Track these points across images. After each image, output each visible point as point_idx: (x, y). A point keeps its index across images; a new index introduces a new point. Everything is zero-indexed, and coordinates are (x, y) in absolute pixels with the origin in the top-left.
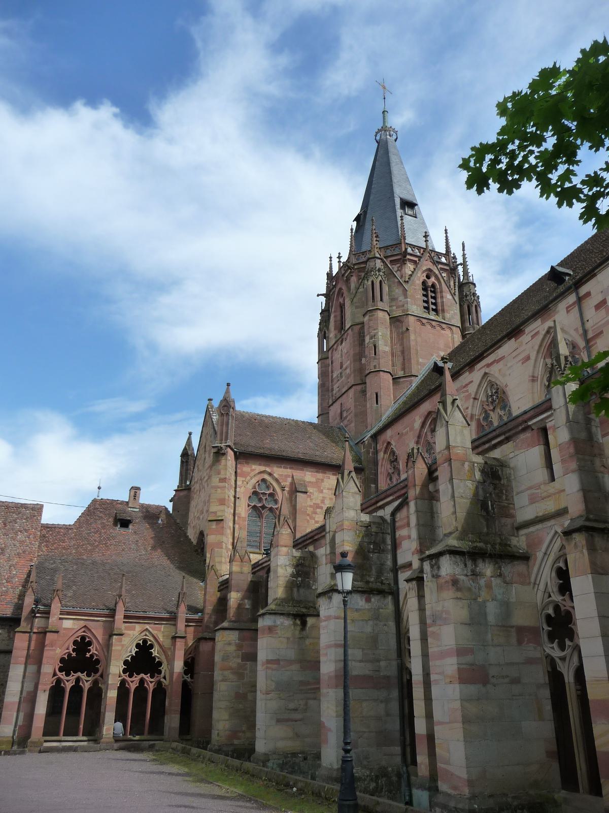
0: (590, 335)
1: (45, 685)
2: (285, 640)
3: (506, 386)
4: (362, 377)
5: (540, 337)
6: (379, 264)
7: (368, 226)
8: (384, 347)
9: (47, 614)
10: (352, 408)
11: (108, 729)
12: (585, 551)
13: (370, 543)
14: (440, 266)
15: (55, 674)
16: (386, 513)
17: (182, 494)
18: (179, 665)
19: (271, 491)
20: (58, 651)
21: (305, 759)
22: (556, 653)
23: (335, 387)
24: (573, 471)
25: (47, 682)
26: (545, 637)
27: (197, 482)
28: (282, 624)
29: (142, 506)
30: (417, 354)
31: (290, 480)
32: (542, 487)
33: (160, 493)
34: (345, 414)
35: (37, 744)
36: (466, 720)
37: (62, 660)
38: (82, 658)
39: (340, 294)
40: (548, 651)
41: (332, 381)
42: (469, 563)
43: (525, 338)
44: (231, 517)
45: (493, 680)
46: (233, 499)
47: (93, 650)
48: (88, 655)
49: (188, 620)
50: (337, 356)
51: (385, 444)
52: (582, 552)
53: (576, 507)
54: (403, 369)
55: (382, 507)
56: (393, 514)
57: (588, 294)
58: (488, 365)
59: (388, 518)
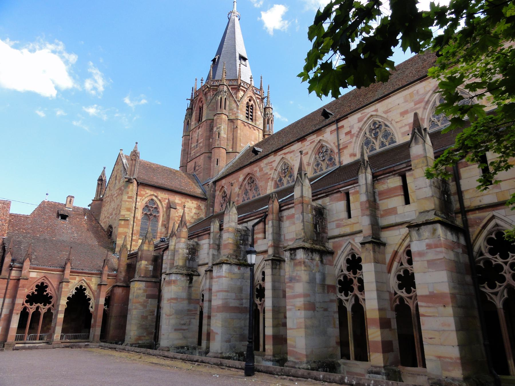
0: (341, 147)
1: (18, 310)
2: (181, 288)
3: (294, 166)
4: (210, 149)
5: (315, 144)
6: (225, 89)
7: (220, 66)
8: (223, 135)
9: (21, 269)
10: (202, 166)
11: (57, 336)
12: (372, 252)
13: (241, 240)
14: (257, 96)
15: (23, 304)
16: (250, 225)
17: (97, 202)
18: (102, 301)
19: (155, 206)
20: (26, 290)
21: (188, 349)
22: (343, 298)
23: (192, 152)
24: (367, 215)
25: (18, 309)
26: (337, 290)
27: (108, 197)
28: (180, 279)
29: (74, 207)
30: (240, 141)
31: (167, 201)
32: (344, 220)
33: (84, 200)
34: (197, 168)
35: (10, 345)
36: (306, 327)
37: (28, 296)
38: (40, 295)
39: (201, 101)
40: (339, 296)
41: (191, 149)
42: (310, 254)
43: (307, 143)
44: (132, 219)
45: (317, 309)
46: (134, 208)
47: (48, 290)
48: (45, 293)
49: (109, 275)
50: (195, 135)
51: (221, 187)
52: (370, 252)
53: (367, 231)
54: (232, 148)
55: (247, 222)
56: (254, 226)
57: (343, 127)
58: (285, 154)
59: (250, 228)
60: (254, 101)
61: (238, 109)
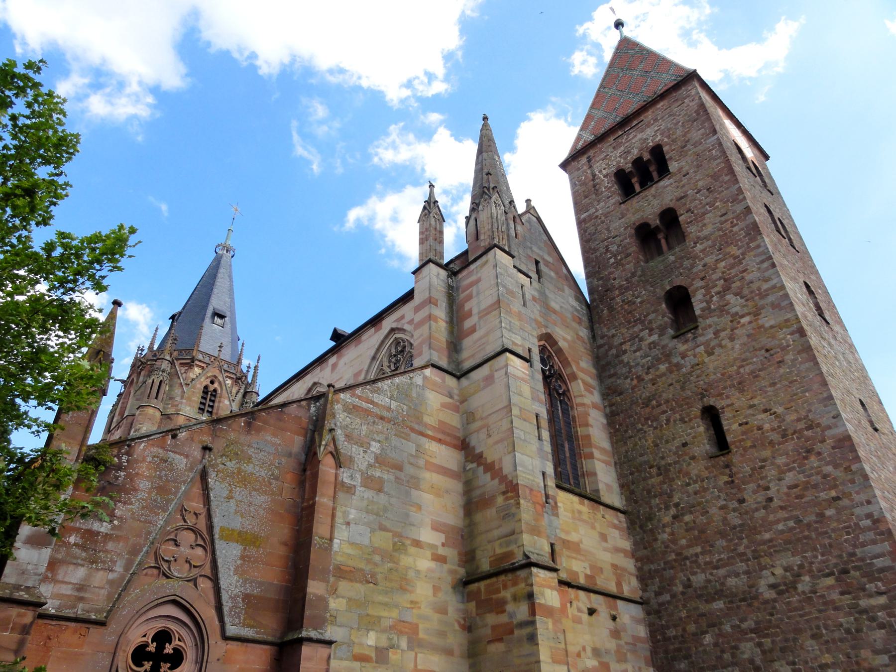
60: (220, 383)
61: (182, 398)
